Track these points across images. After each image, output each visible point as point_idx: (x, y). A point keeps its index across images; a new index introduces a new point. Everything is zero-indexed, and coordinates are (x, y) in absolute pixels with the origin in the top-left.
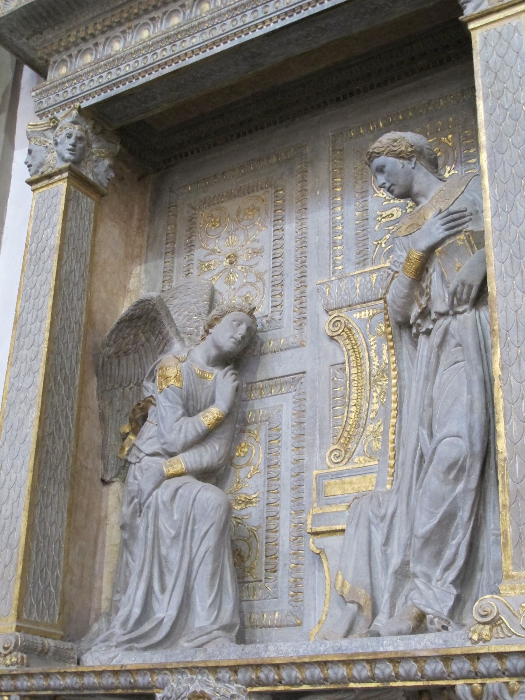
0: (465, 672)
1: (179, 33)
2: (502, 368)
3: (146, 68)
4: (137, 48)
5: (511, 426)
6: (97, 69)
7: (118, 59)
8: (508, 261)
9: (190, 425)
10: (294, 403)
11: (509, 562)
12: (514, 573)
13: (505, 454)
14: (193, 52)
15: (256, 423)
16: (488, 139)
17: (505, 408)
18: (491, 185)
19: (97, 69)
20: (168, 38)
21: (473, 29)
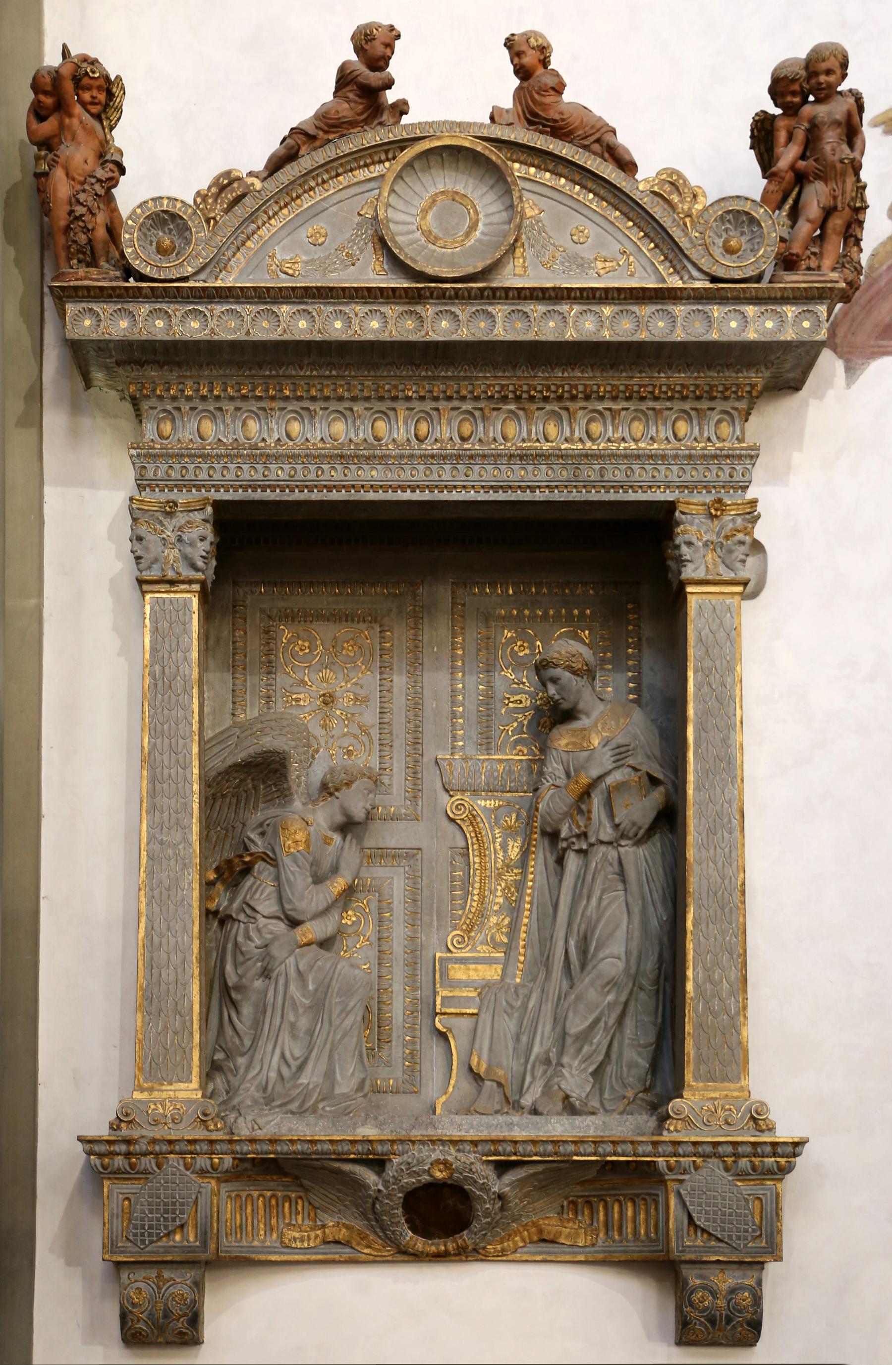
0: (667, 1153)
1: (357, 456)
2: (694, 926)
3: (307, 483)
4: (297, 452)
5: (698, 973)
6: (237, 456)
7: (268, 456)
8: (704, 835)
9: (321, 895)
10: (408, 878)
11: (690, 1075)
12: (694, 1084)
13: (692, 994)
14: (372, 486)
15: (364, 891)
16: (695, 714)
17: (694, 957)
18: (695, 759)
19: (237, 456)
20: (342, 456)
21: (690, 593)
